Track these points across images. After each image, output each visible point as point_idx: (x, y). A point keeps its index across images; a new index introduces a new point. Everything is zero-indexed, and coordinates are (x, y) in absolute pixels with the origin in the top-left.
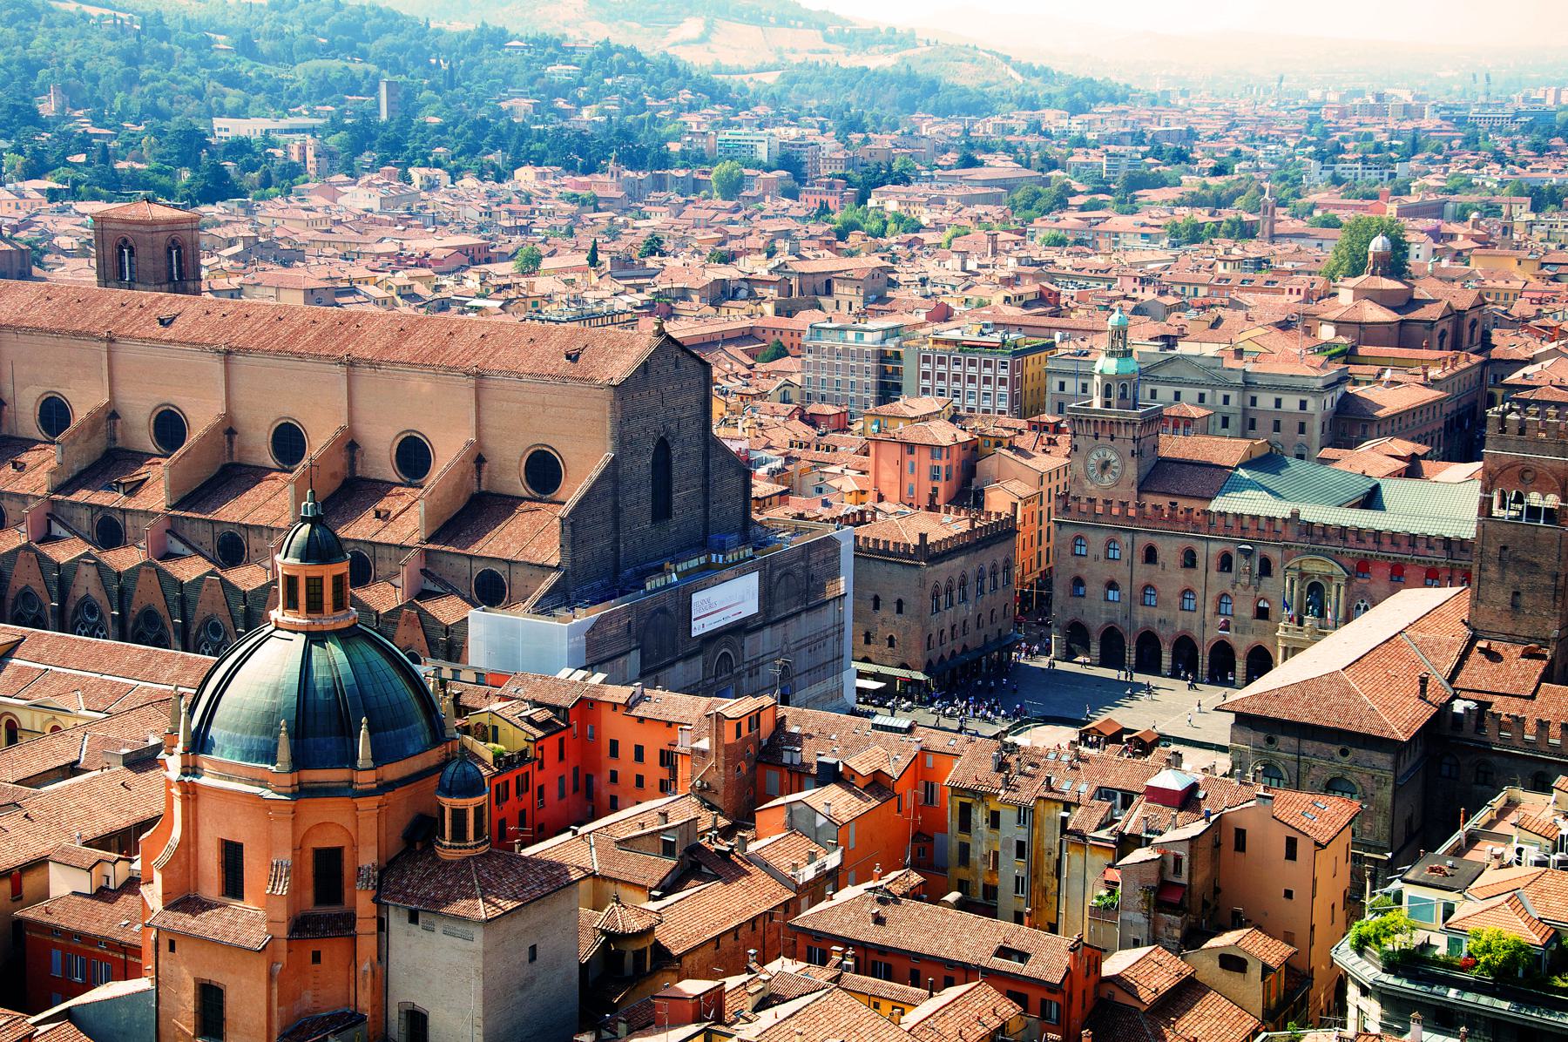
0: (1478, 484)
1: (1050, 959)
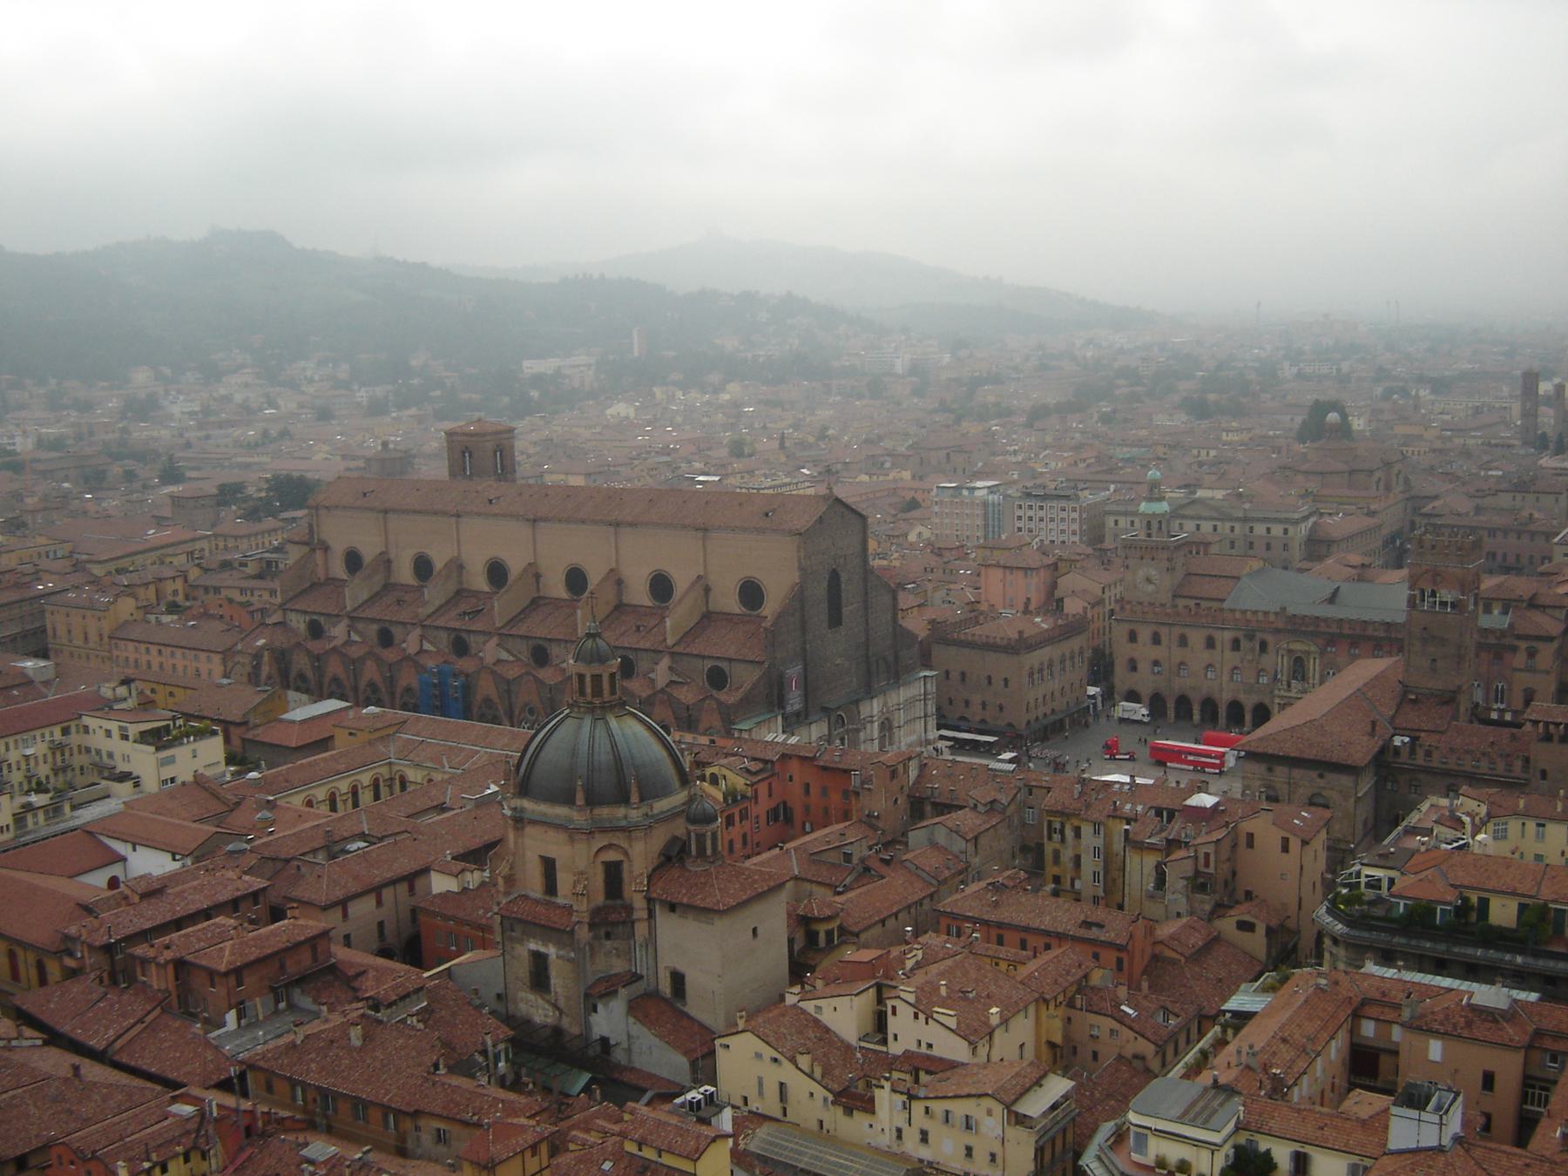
0: (1406, 585)
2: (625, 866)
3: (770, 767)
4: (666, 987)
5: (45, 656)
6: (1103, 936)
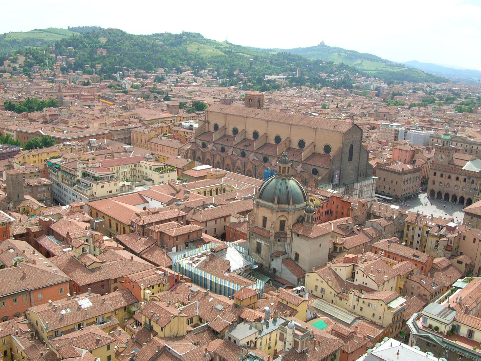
1: (423, 258)
2: (286, 222)
3: (328, 199)
4: (293, 257)
5: (130, 145)
6: (418, 259)
